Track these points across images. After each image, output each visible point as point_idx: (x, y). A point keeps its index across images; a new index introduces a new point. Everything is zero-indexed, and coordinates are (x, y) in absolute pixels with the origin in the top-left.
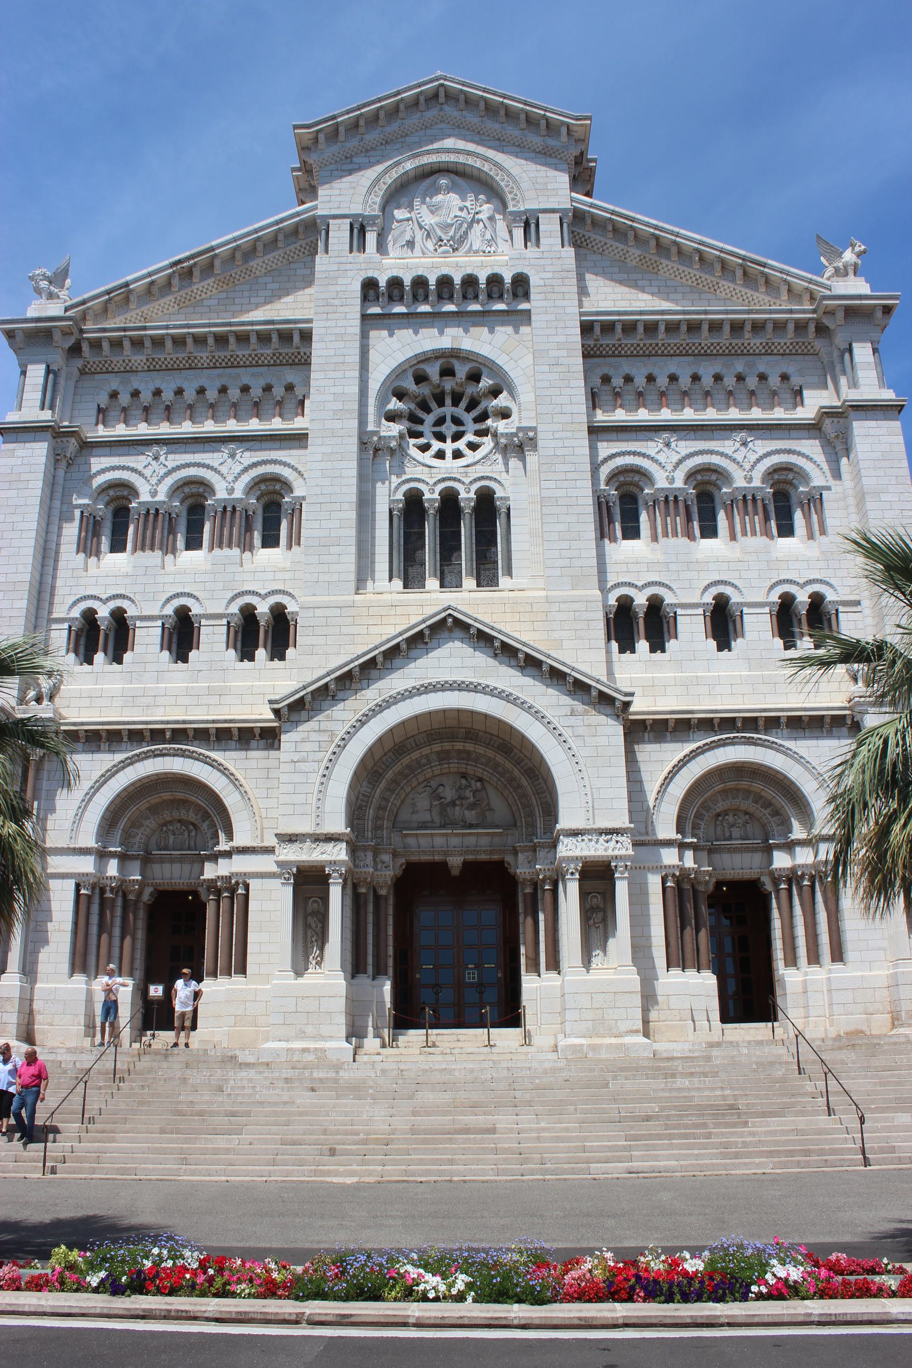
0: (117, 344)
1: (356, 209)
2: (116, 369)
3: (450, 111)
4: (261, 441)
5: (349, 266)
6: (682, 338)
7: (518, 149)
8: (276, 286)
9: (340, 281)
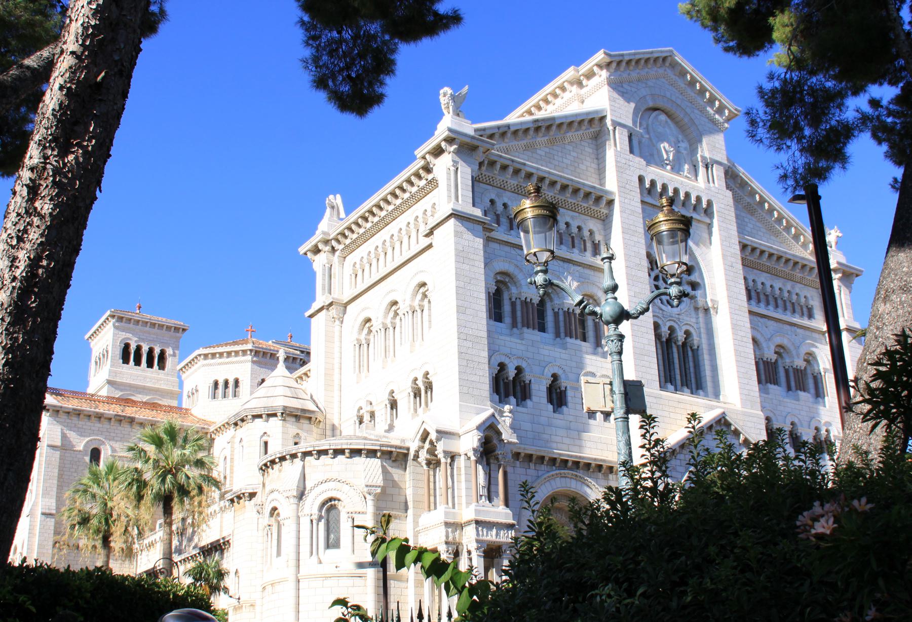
0: (504, 168)
1: (629, 123)
2: (495, 184)
3: (669, 72)
4: (584, 267)
5: (631, 163)
6: (772, 264)
7: (699, 113)
8: (575, 154)
9: (627, 172)
